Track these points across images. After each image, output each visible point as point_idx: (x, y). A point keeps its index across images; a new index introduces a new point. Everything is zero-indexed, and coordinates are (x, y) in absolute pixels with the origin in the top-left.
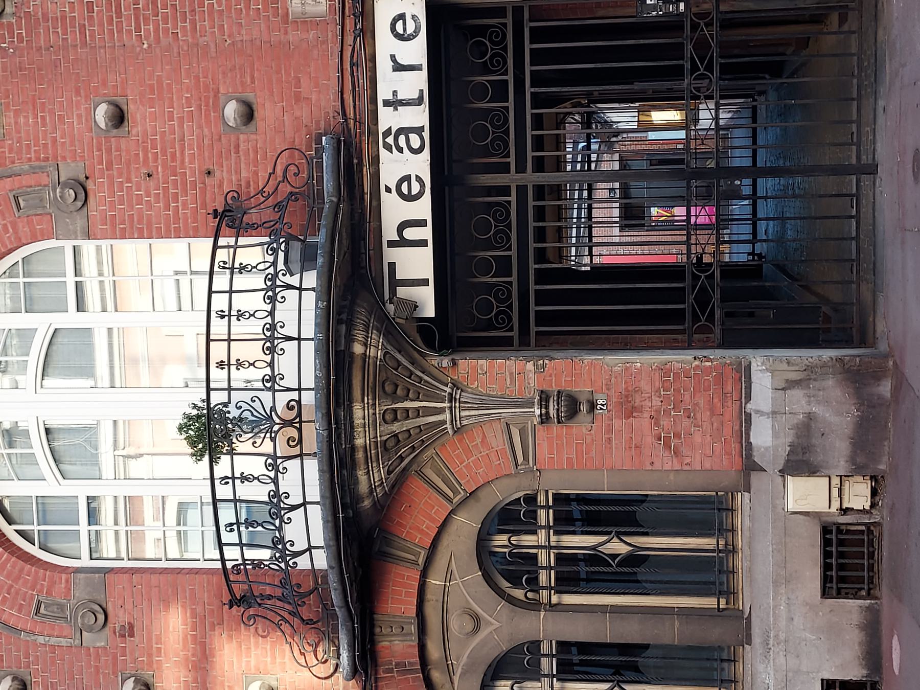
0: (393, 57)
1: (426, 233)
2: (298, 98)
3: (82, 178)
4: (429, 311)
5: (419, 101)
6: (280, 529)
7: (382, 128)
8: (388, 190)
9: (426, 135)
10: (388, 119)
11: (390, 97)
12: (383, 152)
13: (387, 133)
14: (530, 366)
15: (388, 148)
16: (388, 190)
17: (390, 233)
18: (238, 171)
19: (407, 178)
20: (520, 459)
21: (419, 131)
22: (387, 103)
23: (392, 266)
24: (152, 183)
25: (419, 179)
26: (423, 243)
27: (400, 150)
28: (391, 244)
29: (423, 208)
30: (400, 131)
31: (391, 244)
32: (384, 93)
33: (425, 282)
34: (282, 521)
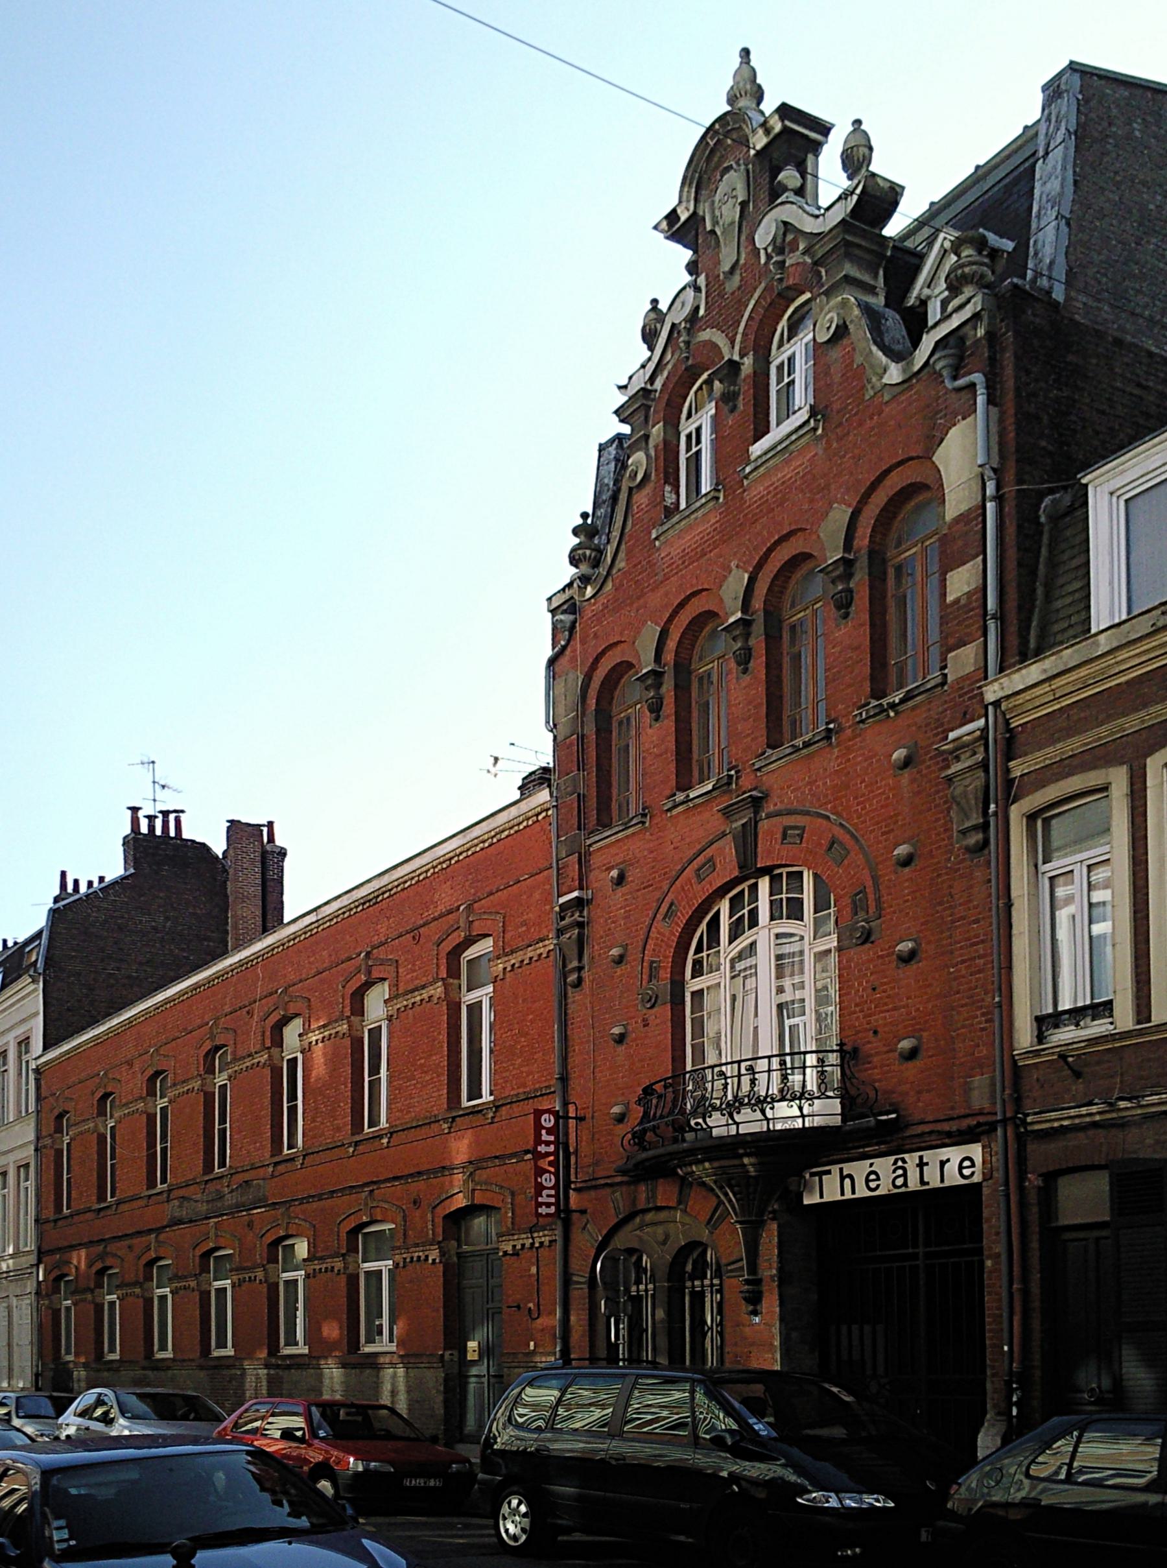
0: (948, 1160)
1: (848, 1195)
2: (919, 1092)
3: (872, 939)
4: (807, 1201)
5: (923, 1182)
6: (749, 1104)
7: (906, 1156)
8: (871, 1165)
9: (903, 1190)
10: (912, 1159)
11: (925, 1160)
12: (892, 1159)
13: (904, 1161)
14: (774, 1272)
15: (895, 1162)
16: (871, 1165)
17: (848, 1168)
18: (877, 1054)
19: (878, 1179)
20: (732, 1267)
21: (905, 1184)
22: (921, 1158)
23: (829, 1172)
24: (870, 991)
25: (878, 1186)
26: (843, 1194)
27: (894, 1171)
28: (841, 1170)
29: (862, 1192)
30: (905, 1169)
31: (841, 1170)
32: (927, 1155)
33: (821, 1196)
34: (754, 1105)
